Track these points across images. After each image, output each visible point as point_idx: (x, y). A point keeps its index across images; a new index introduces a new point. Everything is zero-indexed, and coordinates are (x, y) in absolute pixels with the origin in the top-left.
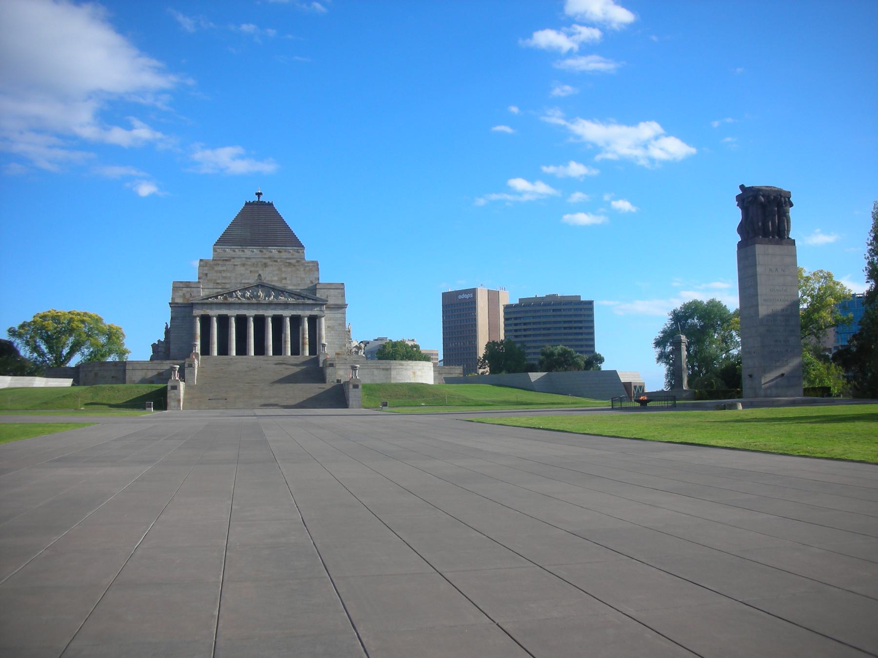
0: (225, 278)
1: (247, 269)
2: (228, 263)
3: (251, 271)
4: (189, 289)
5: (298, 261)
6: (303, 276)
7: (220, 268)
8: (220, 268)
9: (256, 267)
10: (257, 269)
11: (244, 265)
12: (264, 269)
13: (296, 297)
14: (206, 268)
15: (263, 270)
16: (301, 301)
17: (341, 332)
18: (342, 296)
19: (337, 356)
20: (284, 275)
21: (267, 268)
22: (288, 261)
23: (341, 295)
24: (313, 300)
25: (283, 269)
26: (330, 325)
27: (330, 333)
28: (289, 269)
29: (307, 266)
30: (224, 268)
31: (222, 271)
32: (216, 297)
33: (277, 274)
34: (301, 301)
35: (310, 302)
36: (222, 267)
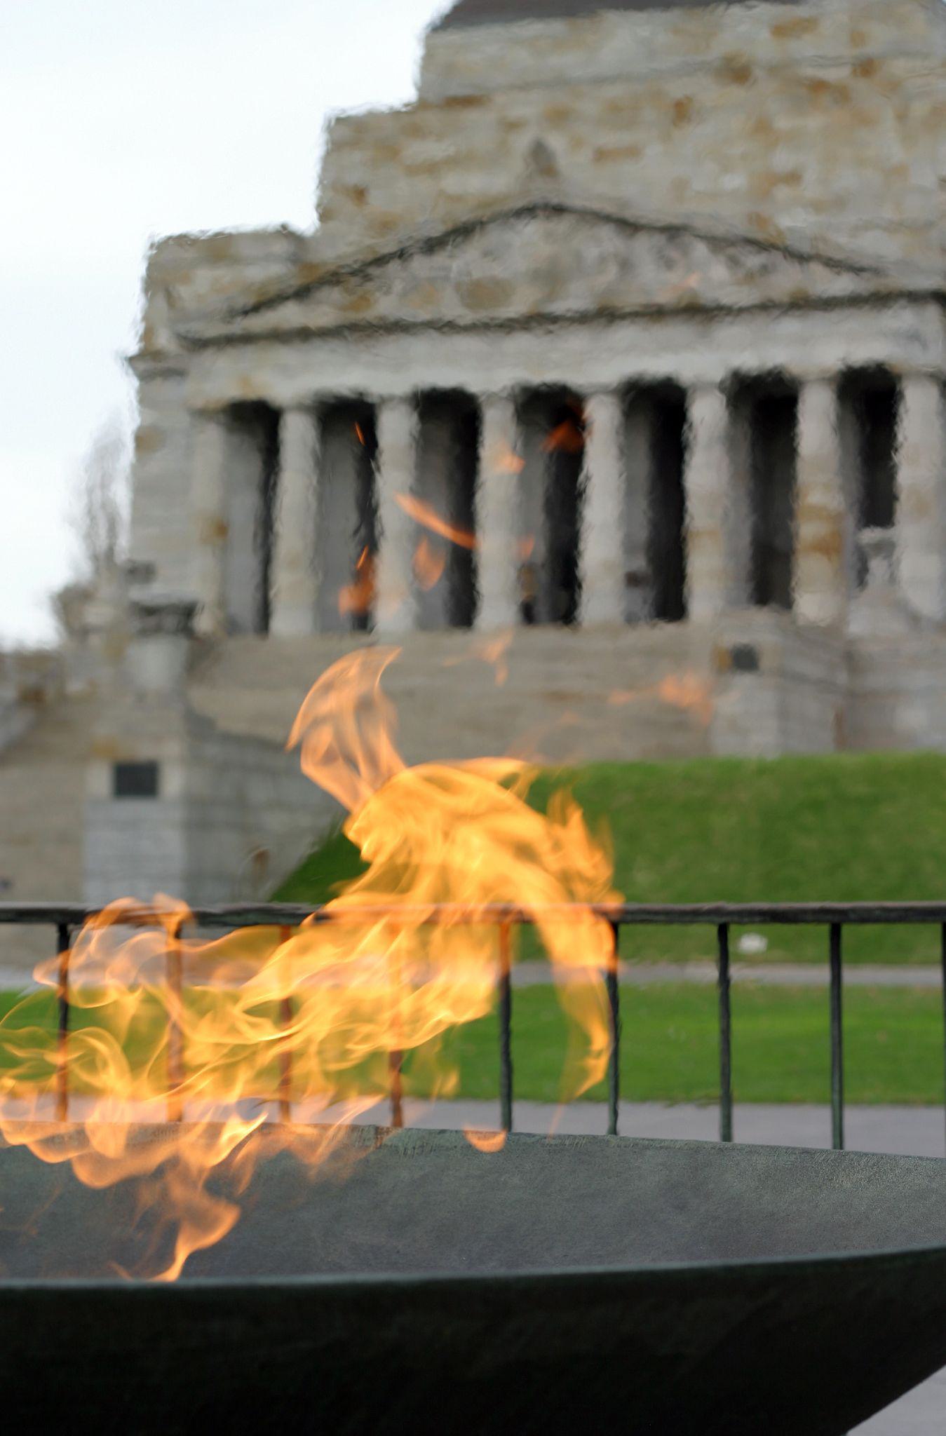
0: (458, 199)
1: (577, 143)
2: (471, 116)
5: (866, 68)
6: (895, 152)
7: (434, 149)
8: (434, 149)
11: (559, 117)
13: (753, 260)
14: (357, 156)
16: (788, 279)
20: (783, 160)
22: (810, 72)
24: (857, 270)
25: (783, 123)
28: (814, 122)
32: (302, 294)
34: (788, 279)
35: (842, 285)
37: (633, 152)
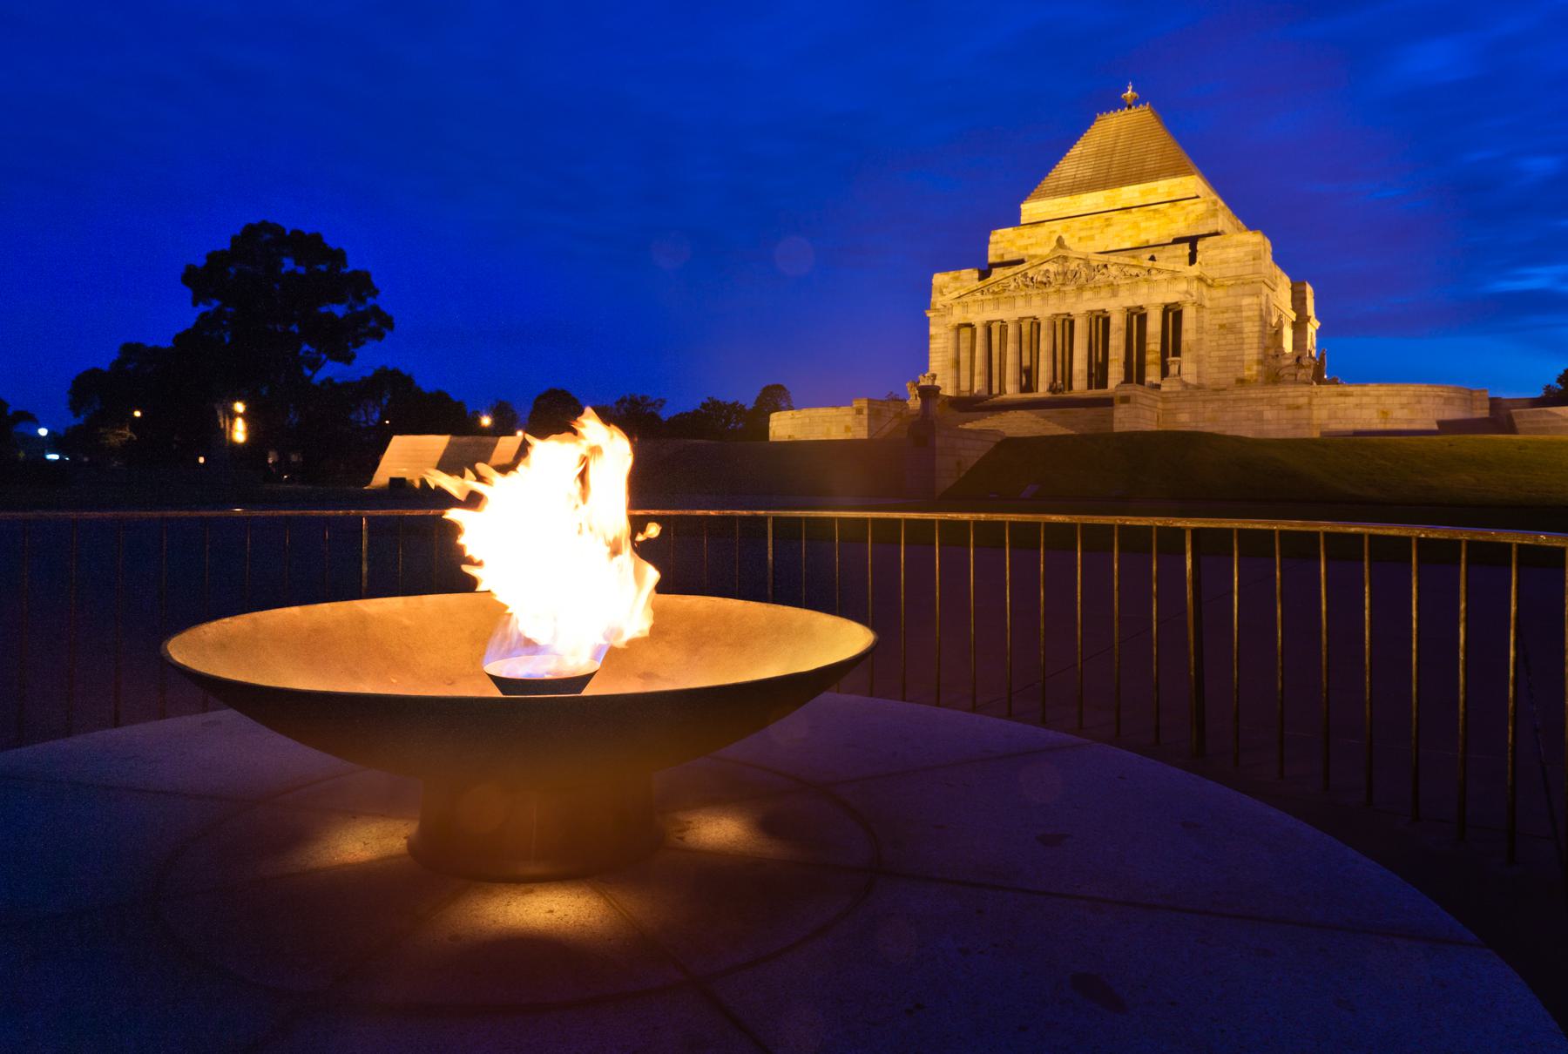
1: (1073, 236)
3: (1080, 239)
4: (958, 285)
9: (1091, 228)
10: (1093, 232)
12: (1105, 229)
15: (1102, 232)
17: (1251, 335)
18: (1254, 259)
19: (1239, 385)
21: (1110, 229)
23: (1251, 258)
25: (1143, 225)
26: (1225, 322)
27: (1225, 339)
28: (1155, 223)
29: (1193, 211)
30: (1033, 240)
31: (1027, 245)
33: (1130, 237)
36: (1029, 238)
37: (1092, 238)
